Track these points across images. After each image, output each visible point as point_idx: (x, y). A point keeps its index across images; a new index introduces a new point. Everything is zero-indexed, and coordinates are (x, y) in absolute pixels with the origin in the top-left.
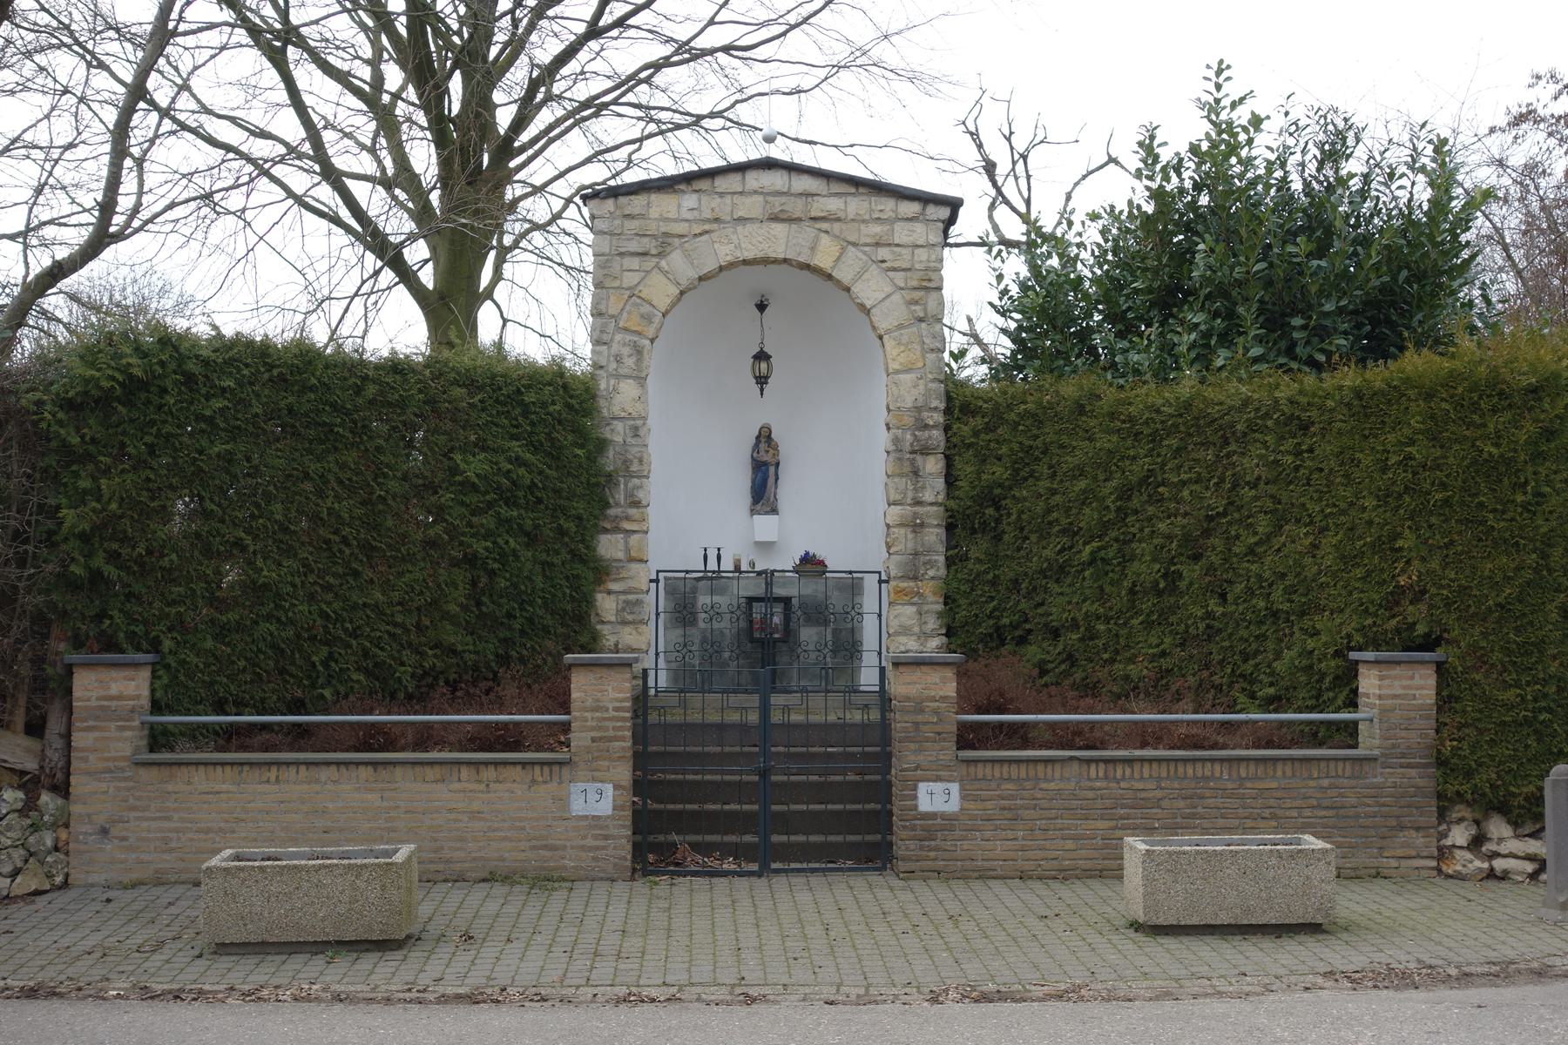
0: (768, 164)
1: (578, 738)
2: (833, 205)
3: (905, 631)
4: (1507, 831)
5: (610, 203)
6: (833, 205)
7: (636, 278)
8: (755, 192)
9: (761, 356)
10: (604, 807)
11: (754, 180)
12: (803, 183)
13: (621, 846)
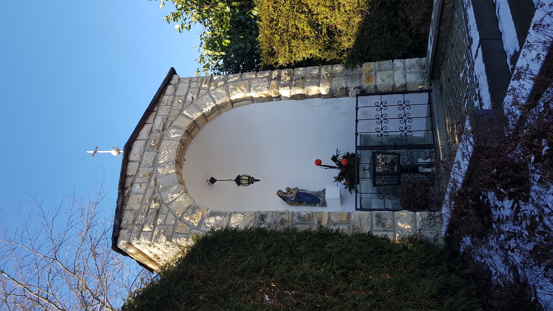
0: (128, 148)
2: (158, 123)
3: (392, 76)
5: (123, 232)
6: (158, 123)
7: (171, 216)
8: (142, 156)
9: (238, 181)
11: (134, 156)
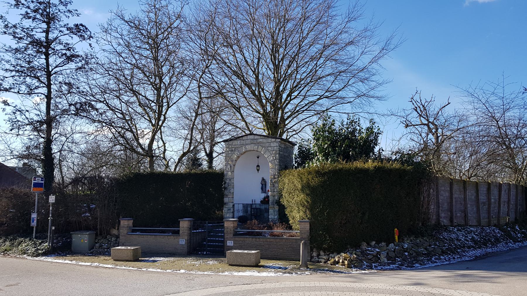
1: (181, 232)
4: (323, 254)
9: (258, 166)
10: (184, 243)
12: (256, 137)
13: (186, 249)
